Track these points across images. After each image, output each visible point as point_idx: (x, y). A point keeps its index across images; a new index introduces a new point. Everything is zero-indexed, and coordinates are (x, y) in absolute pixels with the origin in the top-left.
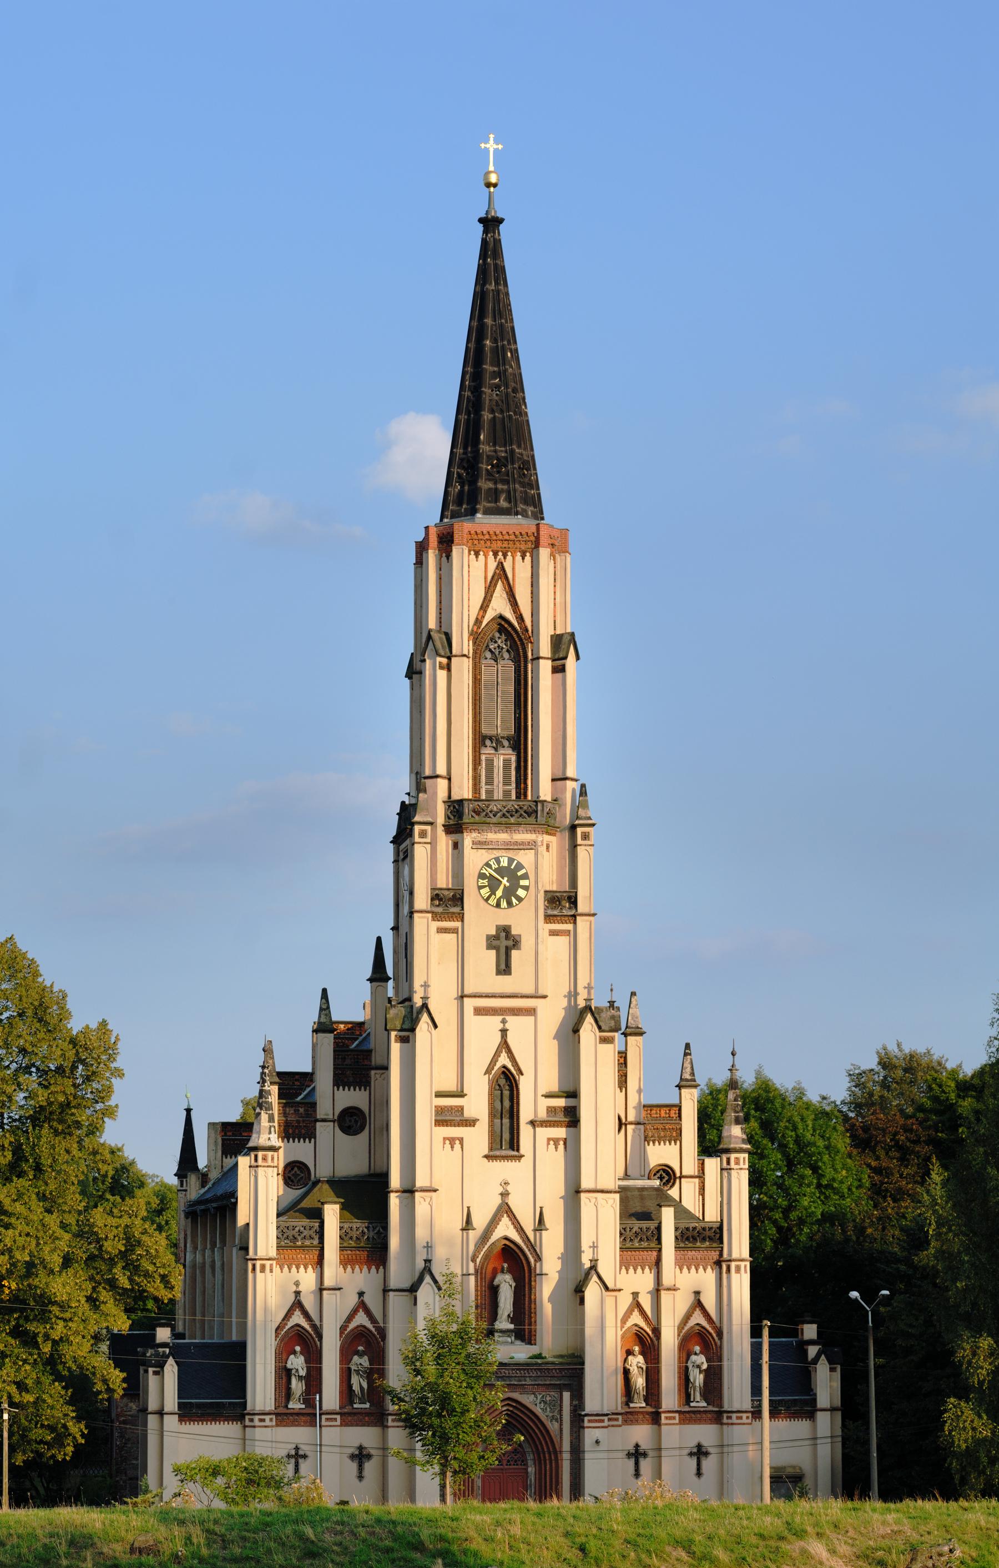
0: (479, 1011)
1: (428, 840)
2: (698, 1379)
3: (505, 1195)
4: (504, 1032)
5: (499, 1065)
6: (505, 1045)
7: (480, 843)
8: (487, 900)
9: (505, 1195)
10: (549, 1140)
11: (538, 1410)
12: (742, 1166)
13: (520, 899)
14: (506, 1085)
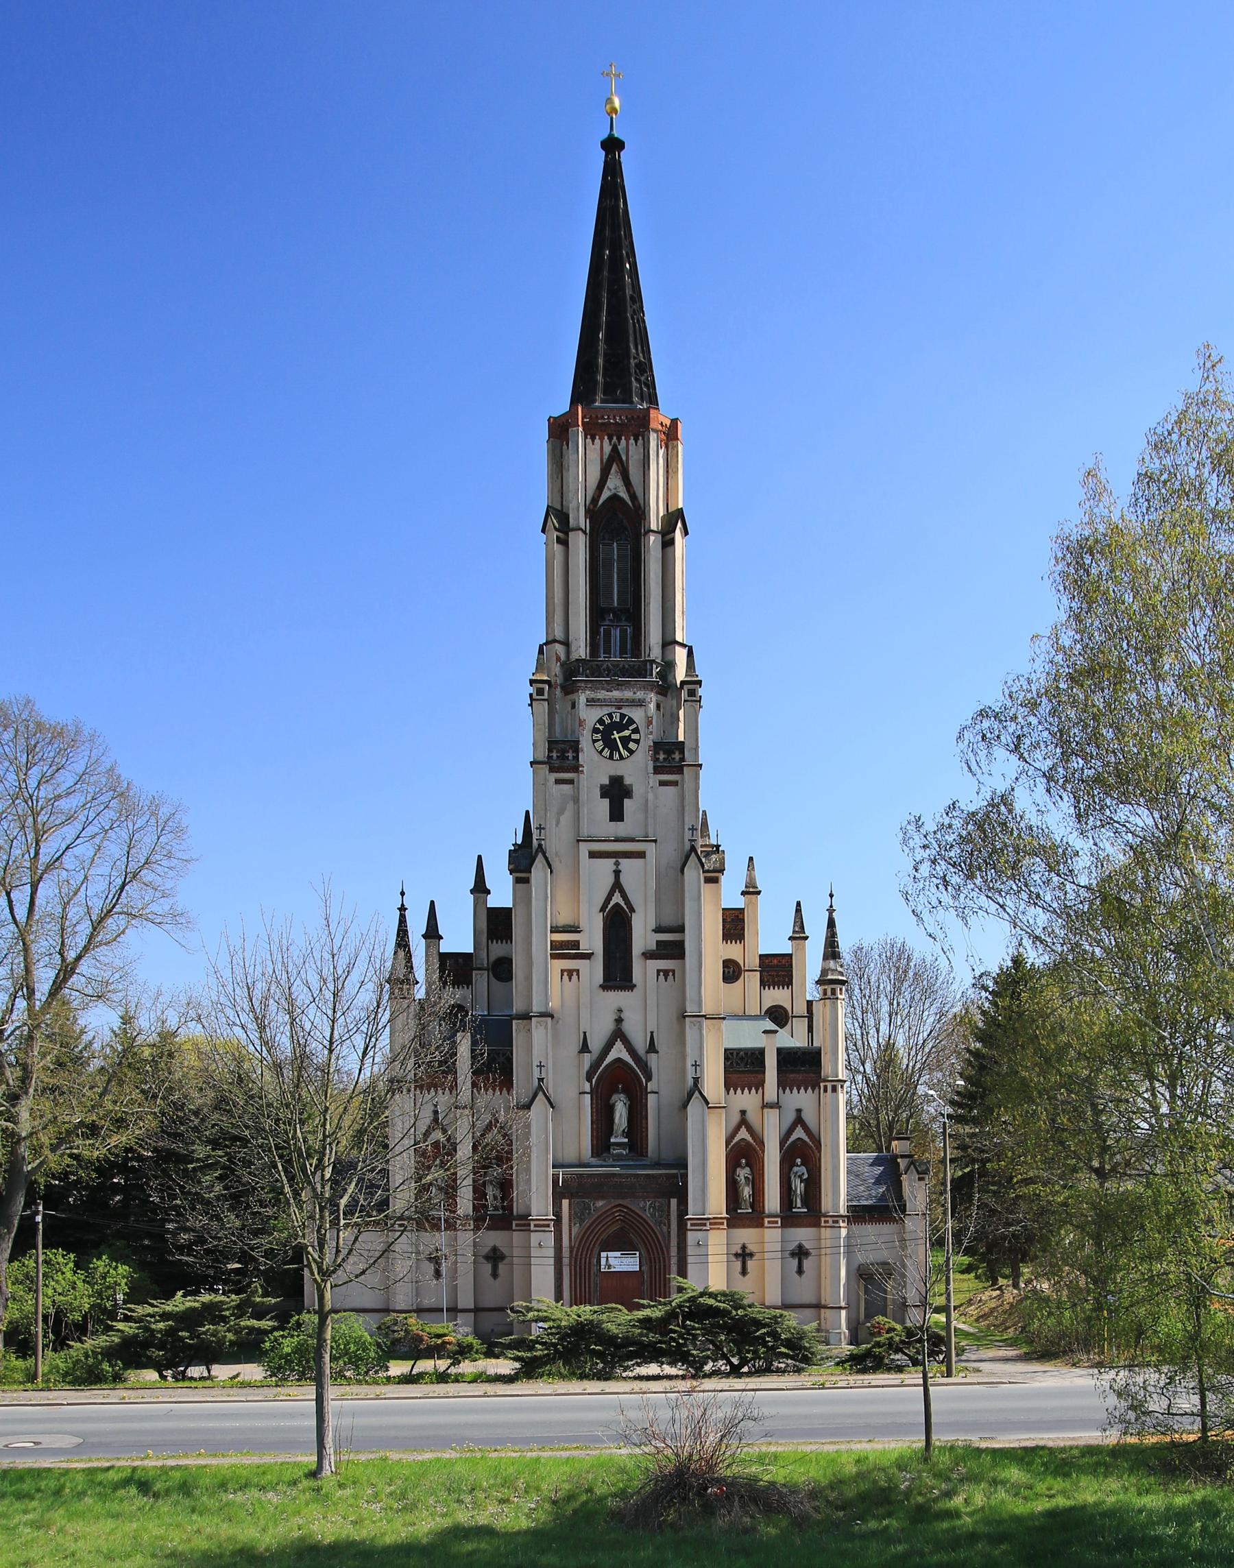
0: (593, 855)
1: (546, 697)
2: (799, 1187)
3: (619, 1021)
4: (617, 873)
5: (612, 903)
6: (617, 886)
7: (593, 700)
8: (601, 752)
9: (619, 1021)
10: (658, 971)
11: (647, 1215)
14: (617, 923)
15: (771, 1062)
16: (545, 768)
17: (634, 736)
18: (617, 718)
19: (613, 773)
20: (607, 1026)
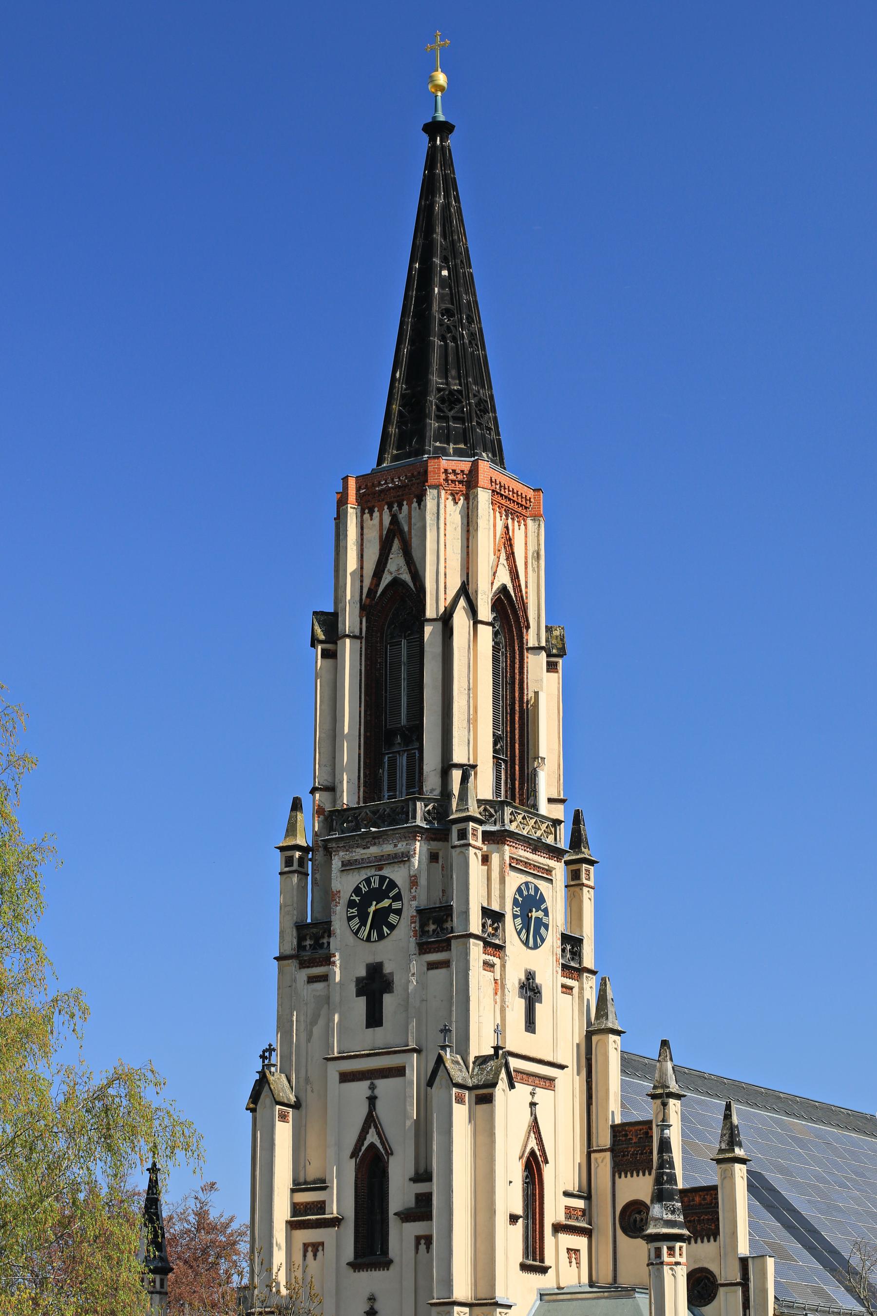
0: (346, 1077)
4: (372, 1100)
5: (366, 1144)
8: (356, 933)
12: (678, 1259)
13: (392, 927)
16: (292, 965)
17: (396, 905)
18: (375, 884)
19: (371, 960)
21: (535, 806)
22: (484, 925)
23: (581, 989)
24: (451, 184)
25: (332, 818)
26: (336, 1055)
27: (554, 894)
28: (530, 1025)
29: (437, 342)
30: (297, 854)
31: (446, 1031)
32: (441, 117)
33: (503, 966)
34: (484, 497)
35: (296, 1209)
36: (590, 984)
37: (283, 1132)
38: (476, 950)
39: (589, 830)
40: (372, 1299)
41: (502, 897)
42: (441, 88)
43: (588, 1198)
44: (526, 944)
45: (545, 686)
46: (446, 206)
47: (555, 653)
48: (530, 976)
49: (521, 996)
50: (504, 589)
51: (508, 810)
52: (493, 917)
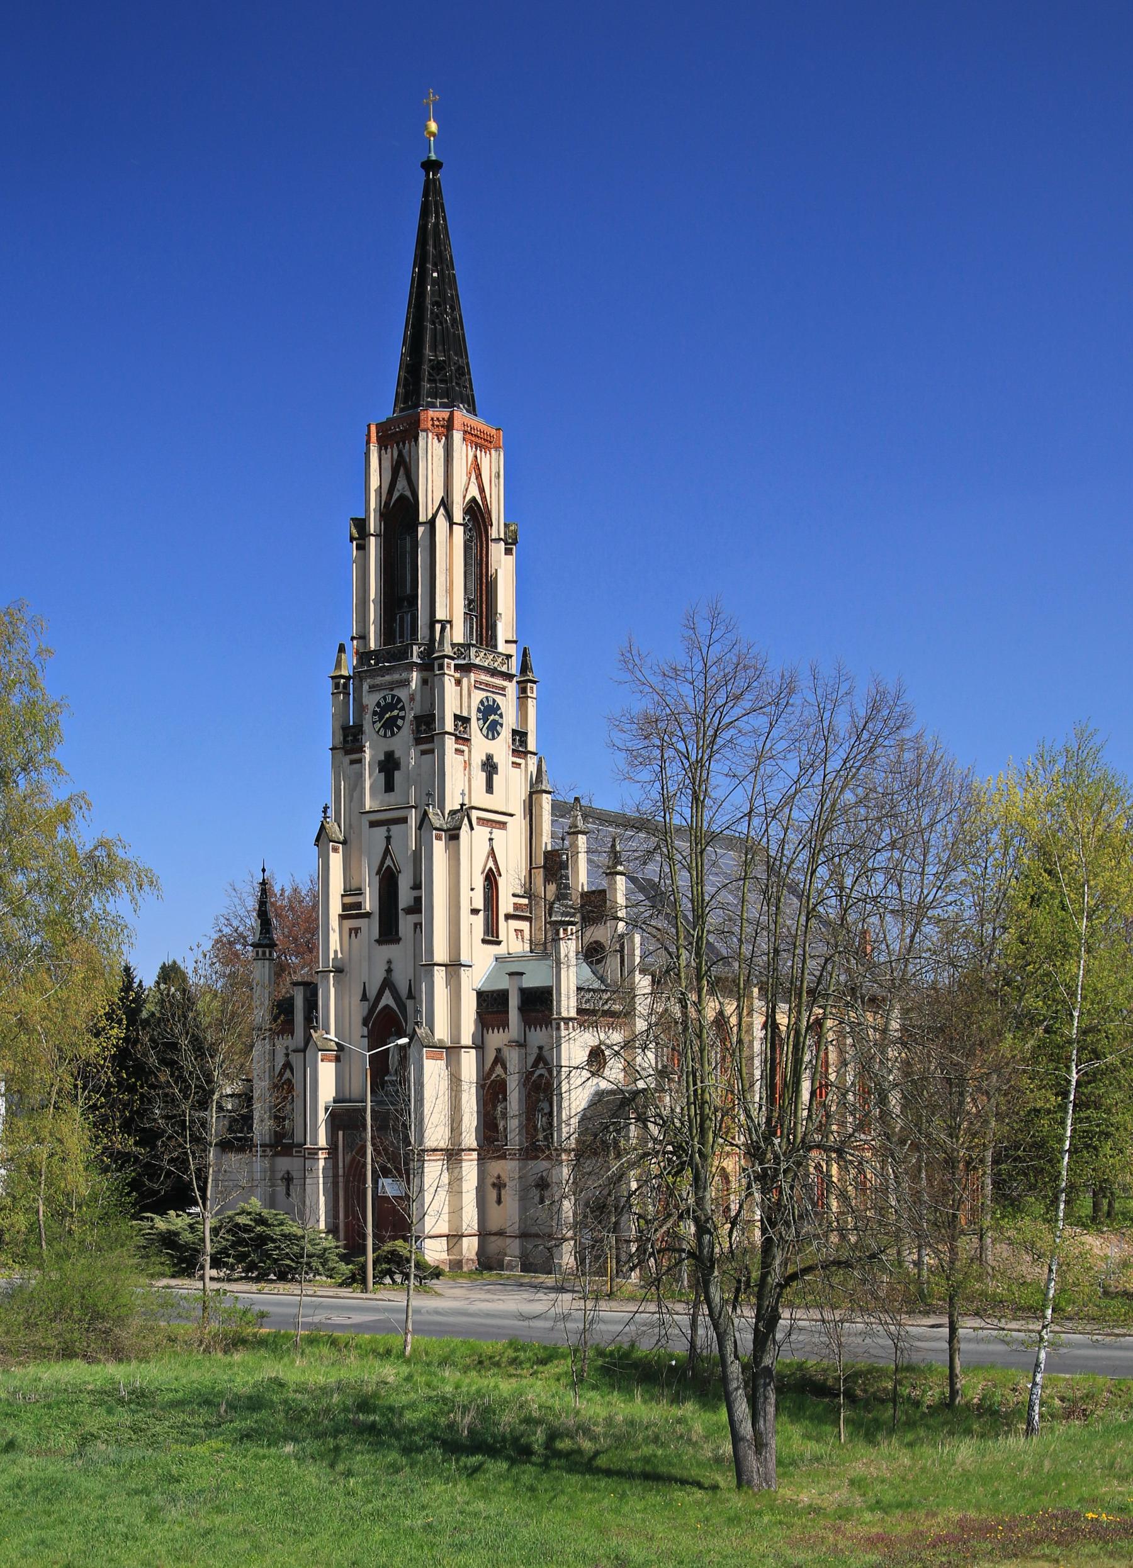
0: (373, 824)
3: (389, 971)
4: (388, 838)
13: (399, 728)
15: (514, 1002)
16: (340, 753)
17: (402, 714)
18: (389, 700)
19: (387, 749)
20: (380, 975)
21: (496, 647)
22: (456, 725)
23: (526, 764)
24: (440, 207)
25: (364, 656)
26: (367, 808)
27: (508, 704)
28: (490, 789)
29: (429, 326)
30: (342, 681)
31: (429, 795)
32: (433, 156)
33: (470, 751)
34: (457, 436)
35: (345, 907)
36: (532, 762)
37: (336, 860)
38: (450, 743)
39: (533, 660)
40: (389, 962)
41: (469, 707)
42: (434, 135)
43: (530, 898)
44: (487, 737)
45: (503, 566)
46: (437, 224)
47: (511, 542)
48: (489, 757)
49: (483, 770)
50: (474, 499)
51: (473, 650)
52: (462, 720)
